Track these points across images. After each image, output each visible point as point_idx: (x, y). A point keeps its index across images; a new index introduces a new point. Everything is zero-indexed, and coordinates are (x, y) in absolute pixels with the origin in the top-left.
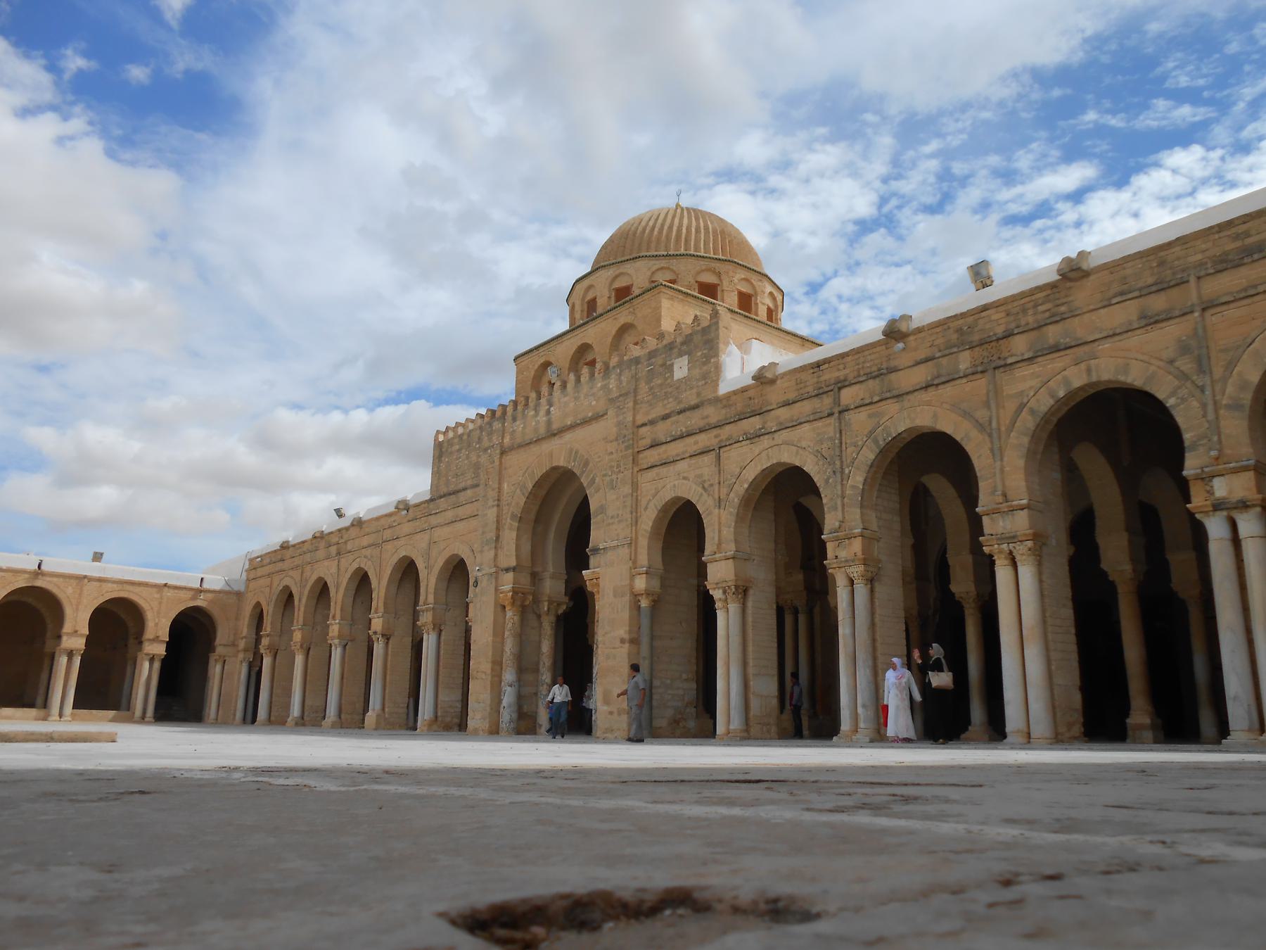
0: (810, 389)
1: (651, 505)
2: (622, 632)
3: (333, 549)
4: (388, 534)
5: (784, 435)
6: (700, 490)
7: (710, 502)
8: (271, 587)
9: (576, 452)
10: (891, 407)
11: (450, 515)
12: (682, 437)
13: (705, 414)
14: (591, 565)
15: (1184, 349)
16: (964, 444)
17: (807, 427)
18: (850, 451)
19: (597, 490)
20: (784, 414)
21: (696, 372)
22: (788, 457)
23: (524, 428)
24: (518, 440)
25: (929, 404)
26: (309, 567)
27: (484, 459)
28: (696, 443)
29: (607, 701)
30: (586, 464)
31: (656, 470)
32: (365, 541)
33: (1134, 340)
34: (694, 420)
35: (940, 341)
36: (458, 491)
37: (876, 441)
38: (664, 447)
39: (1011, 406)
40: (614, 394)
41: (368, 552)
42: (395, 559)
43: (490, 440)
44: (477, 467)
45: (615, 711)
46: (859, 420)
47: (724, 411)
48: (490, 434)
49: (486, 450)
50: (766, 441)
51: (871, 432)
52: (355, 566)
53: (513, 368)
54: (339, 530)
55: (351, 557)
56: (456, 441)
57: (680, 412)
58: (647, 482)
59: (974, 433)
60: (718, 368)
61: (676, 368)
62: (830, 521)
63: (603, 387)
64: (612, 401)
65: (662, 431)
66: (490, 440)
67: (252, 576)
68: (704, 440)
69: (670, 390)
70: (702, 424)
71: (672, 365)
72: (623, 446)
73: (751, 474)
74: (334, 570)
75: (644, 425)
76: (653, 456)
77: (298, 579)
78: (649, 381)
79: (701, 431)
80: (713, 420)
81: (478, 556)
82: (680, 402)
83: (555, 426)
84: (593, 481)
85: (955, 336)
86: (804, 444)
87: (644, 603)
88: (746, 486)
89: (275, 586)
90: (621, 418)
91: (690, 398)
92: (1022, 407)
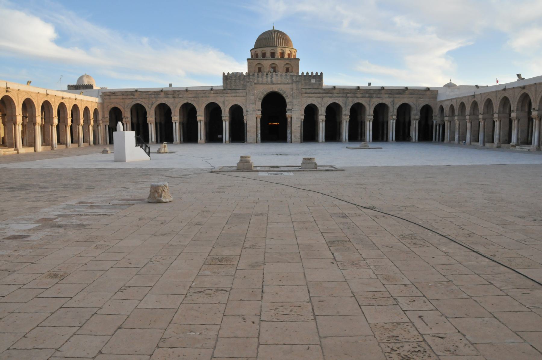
2: (299, 125)
3: (170, 96)
7: (320, 106)
17: (341, 98)
20: (337, 95)
22: (337, 102)
24: (261, 82)
26: (154, 99)
29: (295, 136)
30: (285, 92)
32: (190, 96)
33: (387, 99)
40: (295, 80)
41: (193, 99)
42: (208, 102)
46: (350, 99)
48: (249, 78)
50: (333, 98)
52: (185, 102)
53: (247, 62)
55: (182, 99)
58: (304, 100)
62: (344, 113)
65: (308, 91)
68: (319, 95)
73: (329, 103)
76: (306, 95)
81: (248, 107)
83: (274, 82)
84: (287, 96)
91: (316, 87)
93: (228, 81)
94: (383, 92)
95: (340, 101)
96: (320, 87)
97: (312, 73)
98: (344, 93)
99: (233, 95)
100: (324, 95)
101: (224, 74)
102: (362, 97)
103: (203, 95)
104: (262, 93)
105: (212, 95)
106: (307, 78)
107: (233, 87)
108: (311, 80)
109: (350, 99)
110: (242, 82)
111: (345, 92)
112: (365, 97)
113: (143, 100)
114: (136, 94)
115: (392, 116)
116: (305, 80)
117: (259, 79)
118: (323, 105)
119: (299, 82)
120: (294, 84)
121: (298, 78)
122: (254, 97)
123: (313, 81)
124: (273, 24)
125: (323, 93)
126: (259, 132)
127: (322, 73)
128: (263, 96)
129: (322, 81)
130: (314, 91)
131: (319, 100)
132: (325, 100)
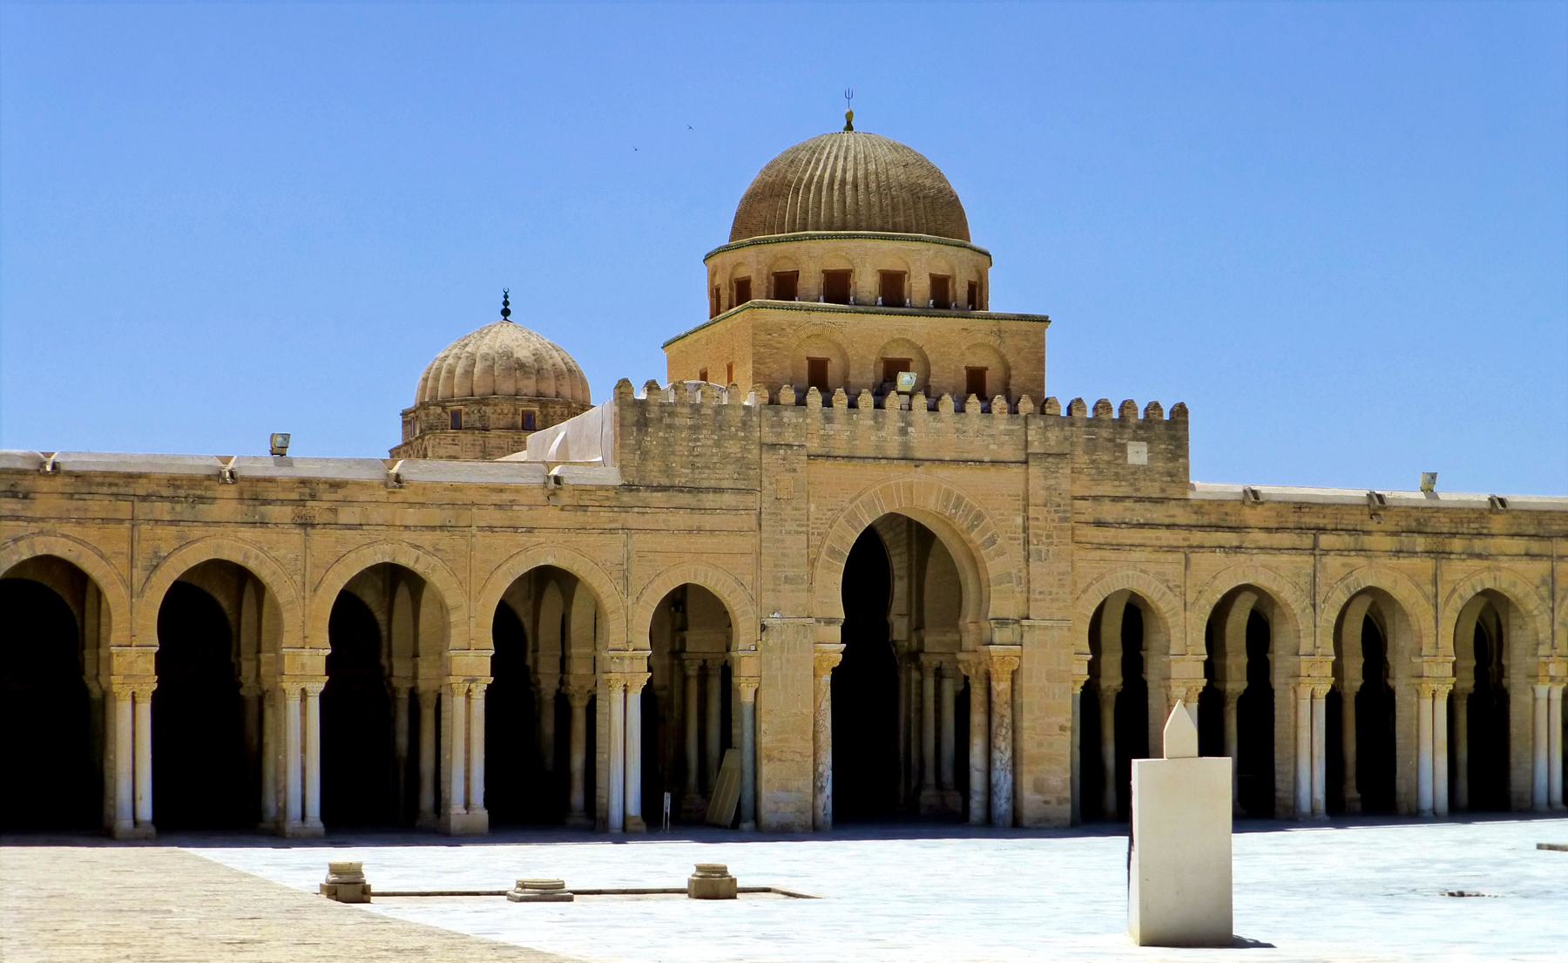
4: (497, 517)
5: (1263, 558)
6: (1163, 588)
9: (959, 499)
12: (1141, 526)
15: (1544, 582)
17: (1284, 558)
18: (1322, 590)
23: (852, 438)
25: (1392, 569)
28: (1158, 538)
30: (979, 517)
31: (1099, 553)
32: (412, 516)
33: (1523, 565)
34: (1158, 514)
35: (1403, 523)
36: (699, 490)
37: (1348, 587)
38: (1113, 530)
39: (1449, 588)
40: (1035, 448)
41: (427, 538)
44: (743, 464)
45: (1054, 801)
50: (1242, 557)
51: (1342, 579)
54: (304, 482)
56: (686, 410)
57: (1140, 500)
59: (1422, 601)
60: (1187, 469)
62: (1306, 645)
63: (1009, 433)
65: (1109, 511)
68: (1167, 537)
70: (1167, 521)
71: (1124, 445)
72: (1056, 516)
75: (1083, 498)
76: (1100, 535)
79: (1168, 526)
80: (1181, 520)
81: (768, 599)
82: (1138, 490)
83: (918, 455)
84: (992, 541)
85: (1414, 524)
87: (1078, 691)
90: (1052, 482)
91: (1153, 490)
92: (1454, 590)
93: (652, 441)
94: (1498, 523)
95: (1277, 572)
96: (1173, 491)
97: (1127, 406)
98: (1301, 529)
99: (682, 519)
100: (1198, 537)
101: (624, 385)
102: (1398, 553)
103: (497, 517)
104: (852, 519)
105: (552, 516)
106: (1105, 433)
107: (683, 476)
108: (1122, 448)
109: (1333, 563)
110: (733, 448)
111: (1308, 523)
112: (1413, 553)
113: (92, 533)
114: (43, 485)
115: (1546, 664)
116: (1092, 447)
117: (831, 429)
118: (1190, 598)
119: (1062, 455)
120: (1035, 470)
121: (1054, 435)
122: (804, 537)
123: (1138, 454)
124: (849, 96)
125: (1189, 527)
126: (826, 759)
127: (1180, 411)
128: (853, 538)
129: (1186, 456)
130: (1141, 513)
131: (1172, 565)
132: (1204, 562)
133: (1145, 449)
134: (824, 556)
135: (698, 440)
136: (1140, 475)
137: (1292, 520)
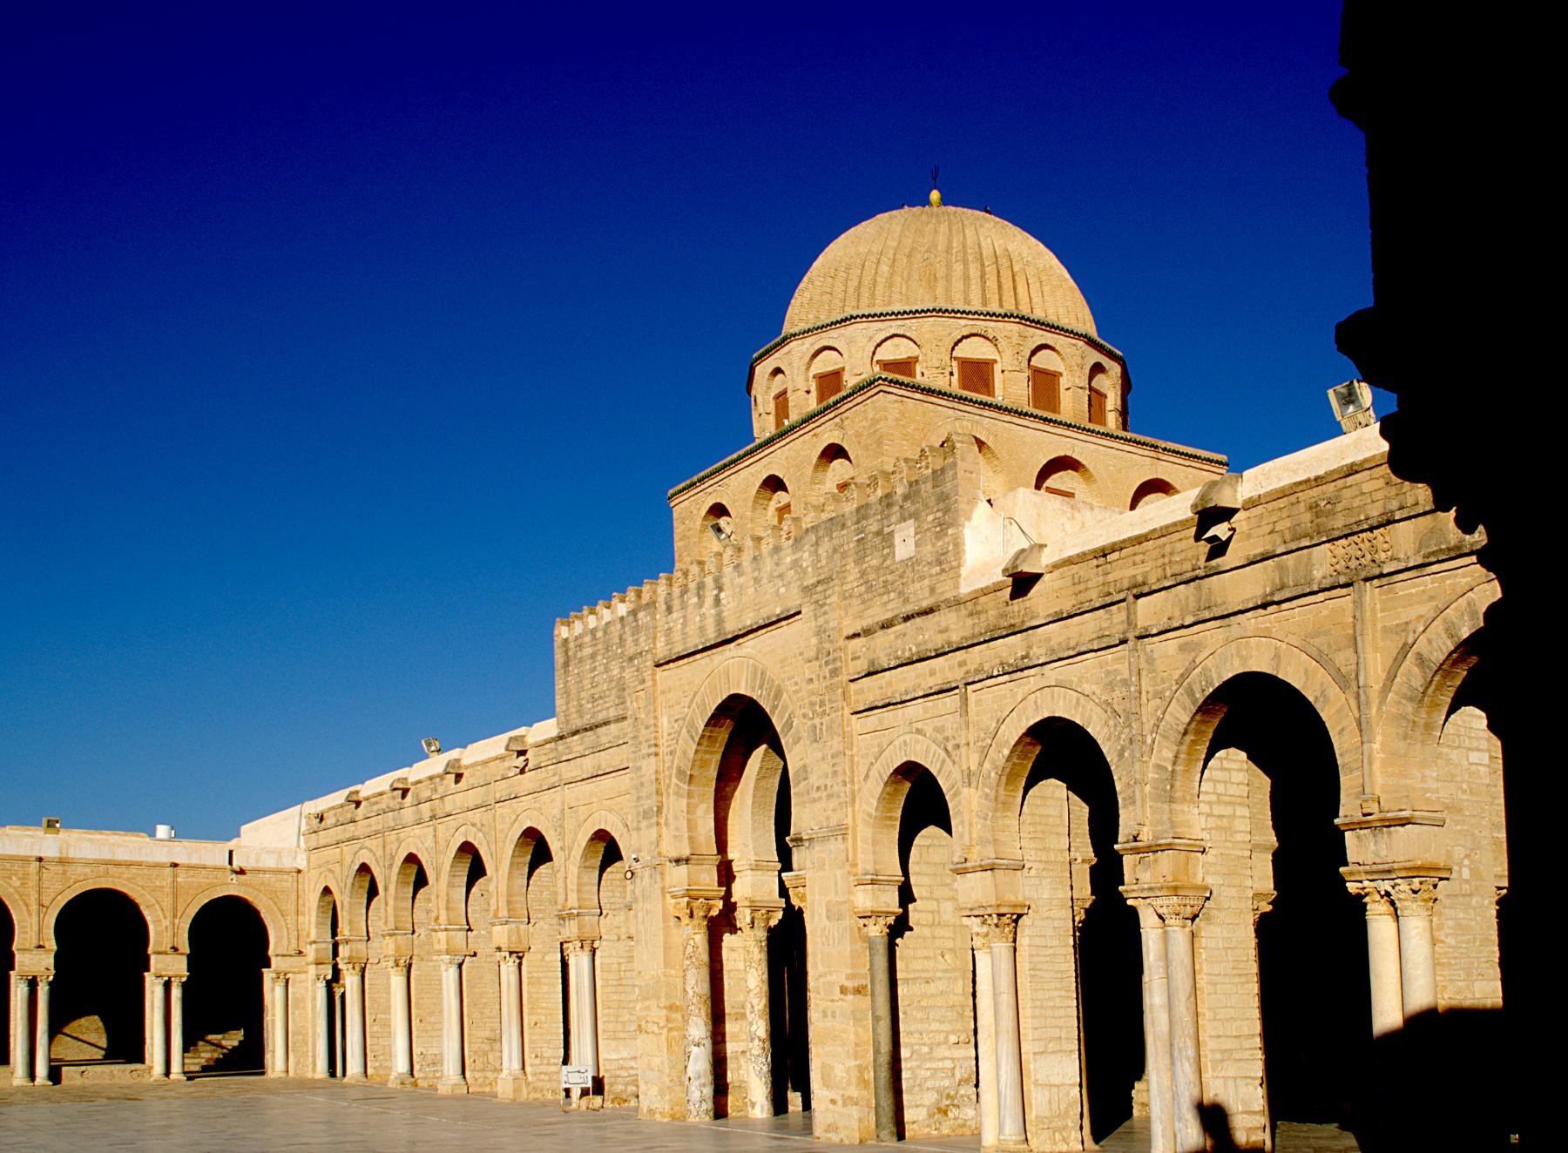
0: (1093, 594)
1: (874, 773)
6: (943, 754)
7: (957, 775)
8: (341, 862)
10: (1211, 635)
11: (588, 765)
13: (943, 624)
14: (795, 866)
16: (1318, 707)
19: (797, 740)
21: (928, 549)
23: (684, 625)
26: (392, 836)
27: (627, 675)
32: (473, 797)
34: (926, 633)
37: (1190, 692)
41: (476, 816)
43: (636, 642)
47: (969, 622)
48: (636, 630)
49: (631, 659)
50: (1033, 679)
51: (1184, 676)
56: (587, 639)
57: (907, 618)
59: (1334, 690)
60: (958, 544)
61: (897, 540)
64: (807, 590)
65: (884, 646)
66: (636, 642)
67: (313, 844)
68: (944, 670)
69: (890, 578)
70: (938, 641)
71: (891, 534)
72: (826, 671)
74: (430, 842)
76: (873, 689)
77: (379, 853)
78: (859, 561)
80: (955, 638)
82: (906, 601)
86: (1087, 688)
88: (1006, 752)
89: (348, 859)
96: (946, 591)
133: (912, 531)
134: (674, 780)
135: (595, 669)
136: (909, 573)
137: (1094, 581)
